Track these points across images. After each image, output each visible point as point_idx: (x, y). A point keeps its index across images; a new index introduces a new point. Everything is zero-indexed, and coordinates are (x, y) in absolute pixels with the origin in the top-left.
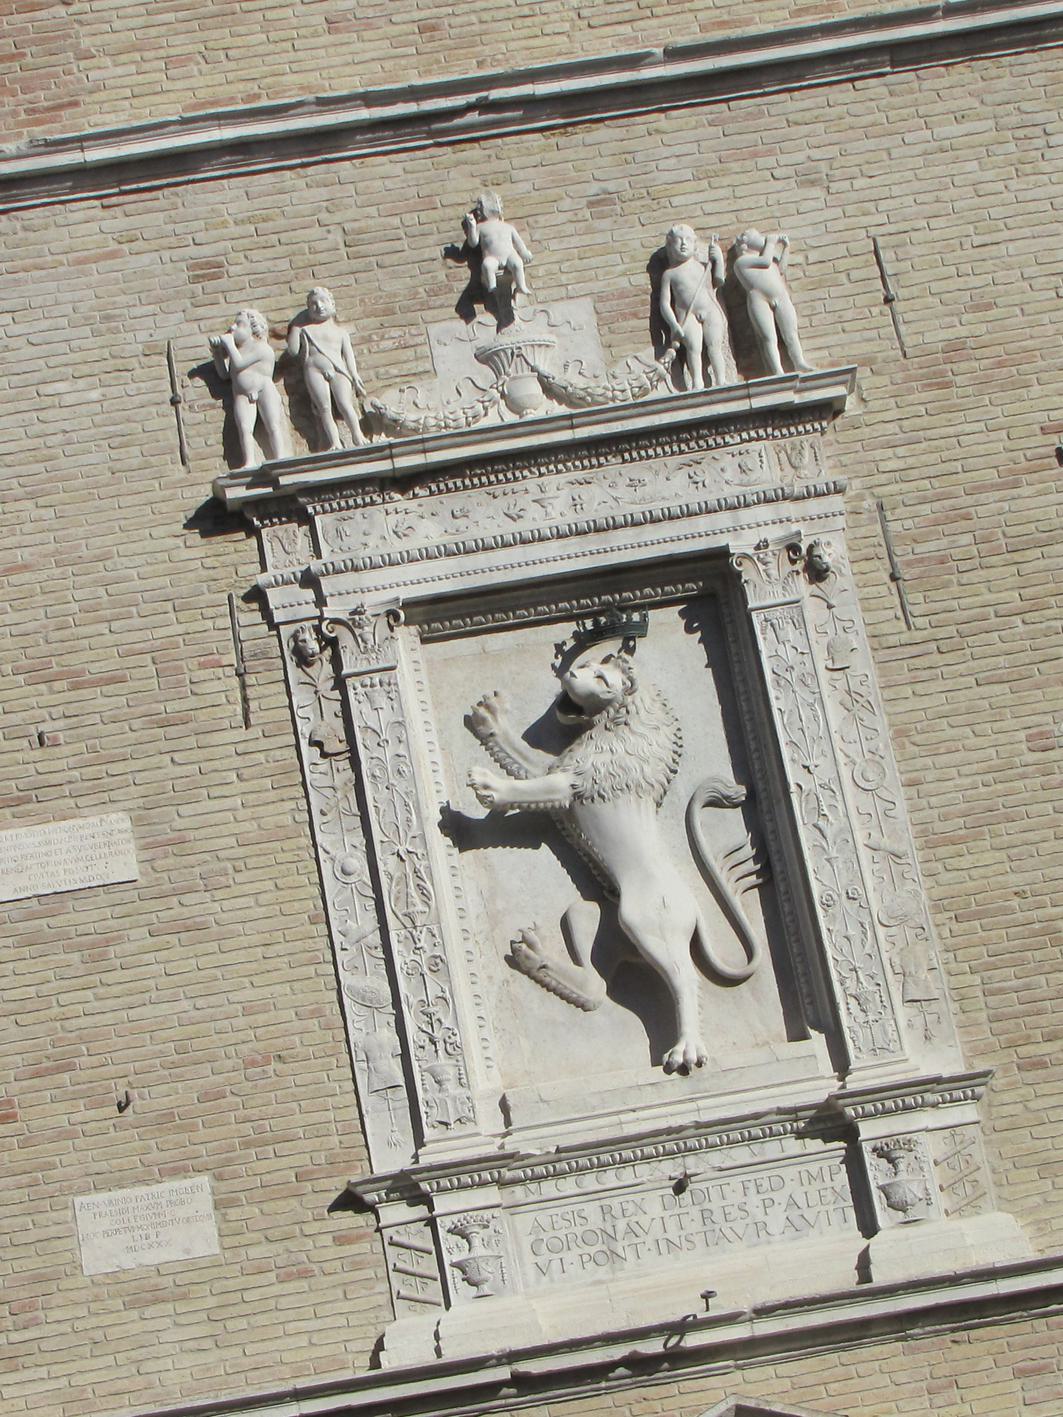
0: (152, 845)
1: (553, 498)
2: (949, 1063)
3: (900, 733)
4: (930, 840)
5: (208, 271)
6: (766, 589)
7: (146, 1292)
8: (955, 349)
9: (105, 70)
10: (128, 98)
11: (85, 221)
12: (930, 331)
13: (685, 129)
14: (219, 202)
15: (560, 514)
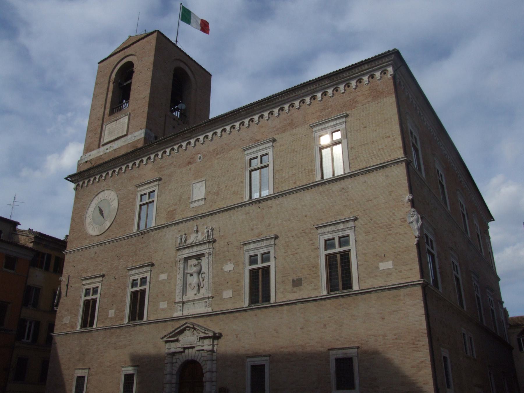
0: (169, 276)
1: (195, 249)
2: (210, 295)
3: (213, 268)
4: (213, 277)
5: (179, 231)
6: (207, 256)
7: (163, 310)
8: (223, 236)
9: (176, 216)
10: (178, 218)
11: (173, 228)
12: (221, 234)
13: (209, 218)
14: (181, 225)
15: (195, 250)
